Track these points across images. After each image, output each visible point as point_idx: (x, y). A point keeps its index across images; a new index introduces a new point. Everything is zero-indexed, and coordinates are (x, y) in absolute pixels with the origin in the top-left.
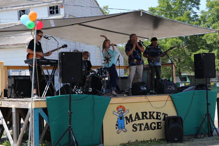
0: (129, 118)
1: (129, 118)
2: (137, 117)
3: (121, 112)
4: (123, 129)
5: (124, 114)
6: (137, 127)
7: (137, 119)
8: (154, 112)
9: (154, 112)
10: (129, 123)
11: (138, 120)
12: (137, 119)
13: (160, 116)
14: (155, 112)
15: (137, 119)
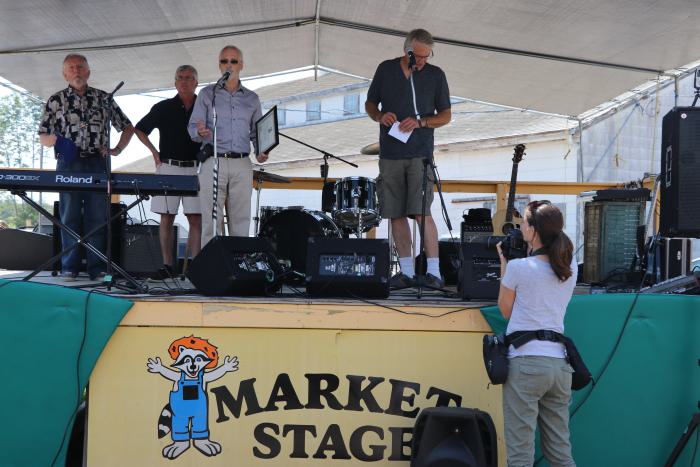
0: (235, 397)
1: (235, 397)
2: (280, 393)
3: (193, 367)
4: (201, 444)
5: (207, 377)
6: (279, 437)
7: (285, 403)
8: (382, 380)
9: (375, 381)
10: (237, 414)
11: (286, 408)
12: (281, 404)
13: (411, 400)
15: (285, 403)
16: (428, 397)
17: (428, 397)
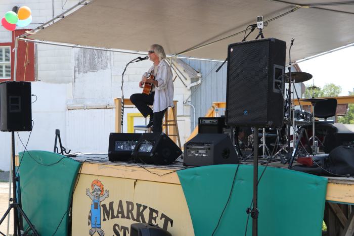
1: (108, 208)
3: (97, 194)
4: (99, 230)
5: (101, 199)
6: (119, 231)
9: (145, 207)
10: (108, 219)
13: (155, 219)
14: (148, 208)
16: (161, 219)
17: (161, 219)
